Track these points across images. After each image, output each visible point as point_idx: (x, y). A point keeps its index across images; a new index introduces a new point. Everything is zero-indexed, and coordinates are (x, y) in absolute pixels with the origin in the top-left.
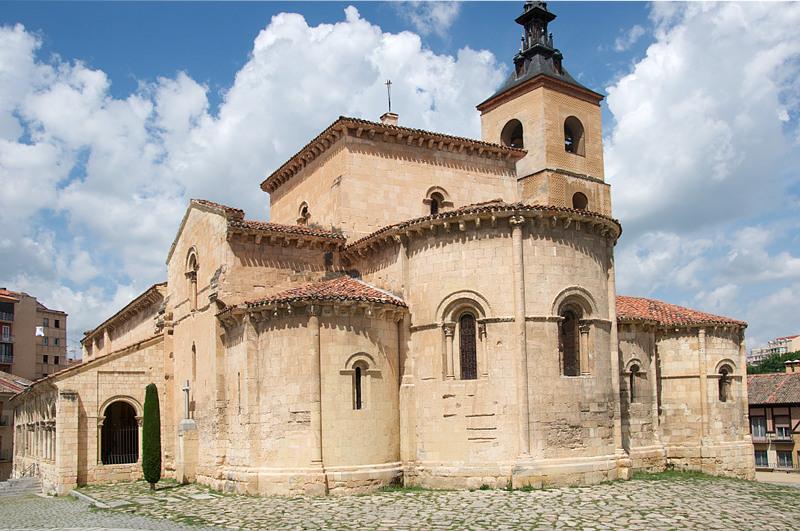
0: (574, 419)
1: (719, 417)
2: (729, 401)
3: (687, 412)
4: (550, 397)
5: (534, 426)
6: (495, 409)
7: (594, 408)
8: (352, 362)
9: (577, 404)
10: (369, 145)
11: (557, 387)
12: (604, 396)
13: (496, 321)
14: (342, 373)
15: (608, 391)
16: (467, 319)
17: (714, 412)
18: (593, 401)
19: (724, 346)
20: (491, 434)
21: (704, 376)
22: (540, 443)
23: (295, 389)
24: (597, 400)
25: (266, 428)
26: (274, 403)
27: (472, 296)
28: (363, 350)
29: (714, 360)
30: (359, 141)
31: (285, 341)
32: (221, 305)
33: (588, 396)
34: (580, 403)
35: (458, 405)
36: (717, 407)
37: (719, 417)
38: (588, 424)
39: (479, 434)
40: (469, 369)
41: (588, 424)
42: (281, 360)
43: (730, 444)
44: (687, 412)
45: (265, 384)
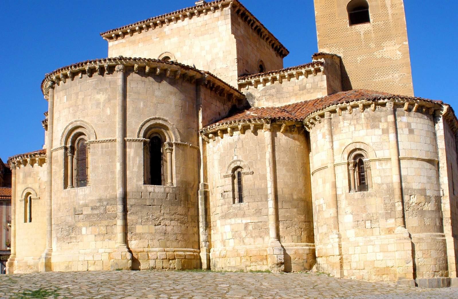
0: (70, 220)
1: (349, 209)
2: (370, 190)
3: (324, 206)
4: (59, 205)
5: (53, 226)
7: (87, 211)
8: (24, 194)
9: (72, 211)
10: (122, 42)
11: (62, 198)
12: (100, 200)
14: (21, 201)
15: (107, 195)
17: (343, 203)
18: (86, 205)
19: (352, 128)
21: (330, 165)
22: (55, 239)
24: (91, 205)
28: (30, 186)
29: (341, 145)
30: (116, 42)
33: (81, 202)
34: (75, 209)
36: (346, 197)
37: (349, 209)
38: (80, 224)
41: (80, 224)
43: (360, 239)
44: (324, 206)
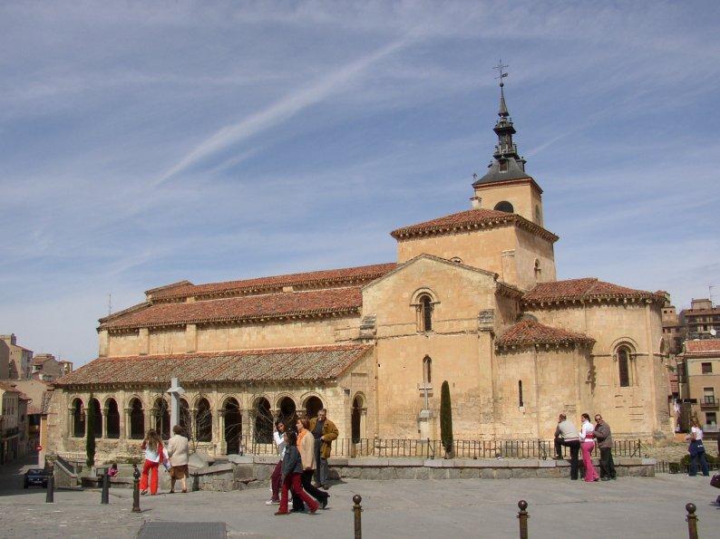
6: (643, 404)
13: (642, 355)
16: (625, 353)
20: (641, 417)
23: (567, 392)
25: (546, 415)
26: (553, 399)
27: (631, 341)
31: (560, 363)
32: (493, 335)
35: (624, 401)
39: (636, 417)
40: (625, 381)
42: (558, 374)
45: (544, 388)
